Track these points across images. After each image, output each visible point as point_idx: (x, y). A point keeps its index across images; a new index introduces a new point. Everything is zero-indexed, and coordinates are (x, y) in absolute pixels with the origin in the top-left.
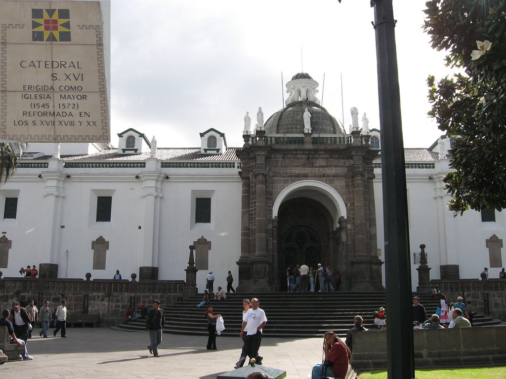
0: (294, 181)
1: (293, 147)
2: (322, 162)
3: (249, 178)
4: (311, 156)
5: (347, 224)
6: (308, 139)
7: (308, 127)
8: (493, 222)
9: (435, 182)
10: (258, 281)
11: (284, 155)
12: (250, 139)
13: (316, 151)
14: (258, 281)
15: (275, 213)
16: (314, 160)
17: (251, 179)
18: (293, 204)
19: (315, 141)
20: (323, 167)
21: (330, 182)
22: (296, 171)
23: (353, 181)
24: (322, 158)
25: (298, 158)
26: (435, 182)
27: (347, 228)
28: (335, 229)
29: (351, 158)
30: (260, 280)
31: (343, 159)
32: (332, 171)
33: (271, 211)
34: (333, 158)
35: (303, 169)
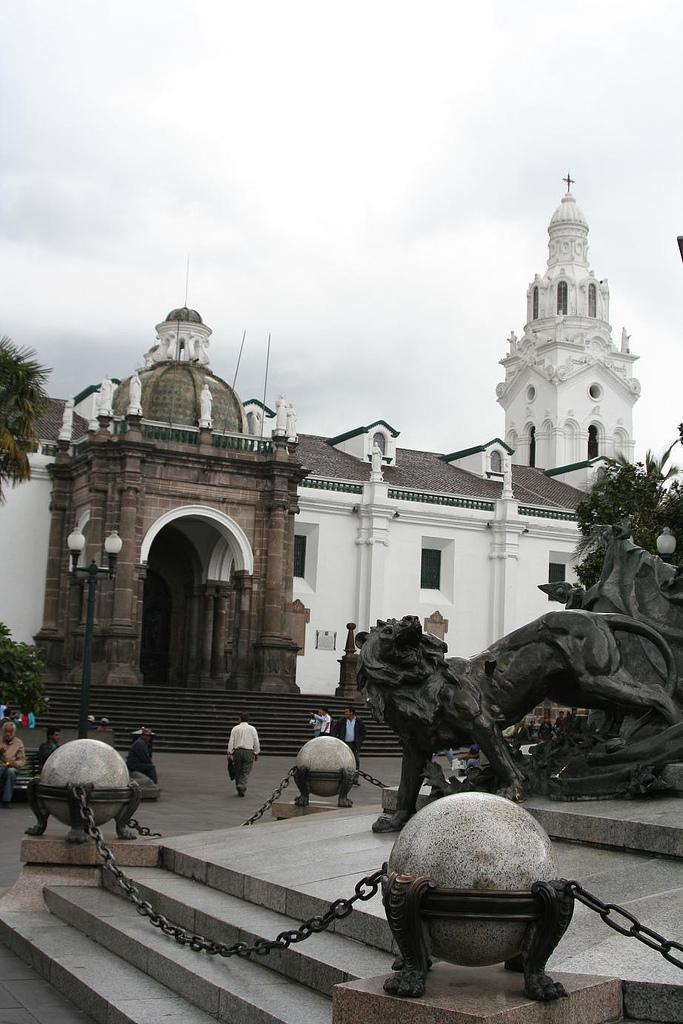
0: (178, 504)
1: (181, 447)
2: (223, 479)
3: (106, 492)
5: (252, 583)
6: (205, 437)
7: (206, 420)
8: (435, 591)
9: (360, 518)
10: (117, 666)
11: (168, 459)
12: (111, 424)
13: (218, 460)
14: (117, 666)
15: (144, 556)
16: (212, 474)
17: (110, 493)
19: (218, 442)
20: (226, 487)
21: (233, 513)
22: (183, 488)
23: (269, 516)
24: (225, 472)
25: (187, 467)
26: (360, 518)
27: (251, 589)
28: (204, 582)
29: (271, 478)
30: (121, 665)
31: (256, 477)
32: (238, 495)
33: (139, 551)
34: (241, 474)
35: (195, 486)
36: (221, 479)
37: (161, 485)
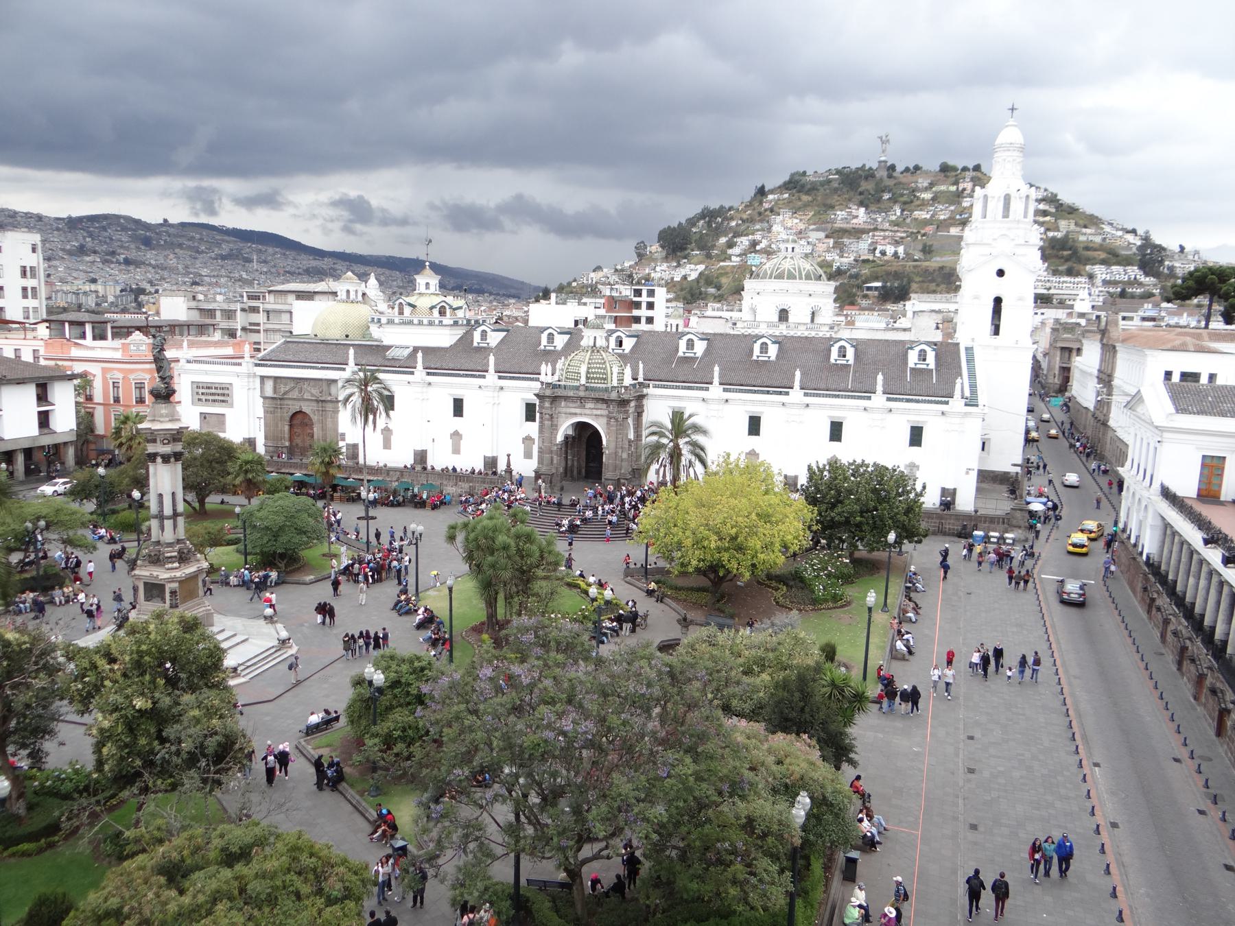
4: (582, 400)
15: (560, 438)
18: (582, 427)
22: (573, 410)
32: (599, 412)
36: (590, 405)
37: (564, 410)
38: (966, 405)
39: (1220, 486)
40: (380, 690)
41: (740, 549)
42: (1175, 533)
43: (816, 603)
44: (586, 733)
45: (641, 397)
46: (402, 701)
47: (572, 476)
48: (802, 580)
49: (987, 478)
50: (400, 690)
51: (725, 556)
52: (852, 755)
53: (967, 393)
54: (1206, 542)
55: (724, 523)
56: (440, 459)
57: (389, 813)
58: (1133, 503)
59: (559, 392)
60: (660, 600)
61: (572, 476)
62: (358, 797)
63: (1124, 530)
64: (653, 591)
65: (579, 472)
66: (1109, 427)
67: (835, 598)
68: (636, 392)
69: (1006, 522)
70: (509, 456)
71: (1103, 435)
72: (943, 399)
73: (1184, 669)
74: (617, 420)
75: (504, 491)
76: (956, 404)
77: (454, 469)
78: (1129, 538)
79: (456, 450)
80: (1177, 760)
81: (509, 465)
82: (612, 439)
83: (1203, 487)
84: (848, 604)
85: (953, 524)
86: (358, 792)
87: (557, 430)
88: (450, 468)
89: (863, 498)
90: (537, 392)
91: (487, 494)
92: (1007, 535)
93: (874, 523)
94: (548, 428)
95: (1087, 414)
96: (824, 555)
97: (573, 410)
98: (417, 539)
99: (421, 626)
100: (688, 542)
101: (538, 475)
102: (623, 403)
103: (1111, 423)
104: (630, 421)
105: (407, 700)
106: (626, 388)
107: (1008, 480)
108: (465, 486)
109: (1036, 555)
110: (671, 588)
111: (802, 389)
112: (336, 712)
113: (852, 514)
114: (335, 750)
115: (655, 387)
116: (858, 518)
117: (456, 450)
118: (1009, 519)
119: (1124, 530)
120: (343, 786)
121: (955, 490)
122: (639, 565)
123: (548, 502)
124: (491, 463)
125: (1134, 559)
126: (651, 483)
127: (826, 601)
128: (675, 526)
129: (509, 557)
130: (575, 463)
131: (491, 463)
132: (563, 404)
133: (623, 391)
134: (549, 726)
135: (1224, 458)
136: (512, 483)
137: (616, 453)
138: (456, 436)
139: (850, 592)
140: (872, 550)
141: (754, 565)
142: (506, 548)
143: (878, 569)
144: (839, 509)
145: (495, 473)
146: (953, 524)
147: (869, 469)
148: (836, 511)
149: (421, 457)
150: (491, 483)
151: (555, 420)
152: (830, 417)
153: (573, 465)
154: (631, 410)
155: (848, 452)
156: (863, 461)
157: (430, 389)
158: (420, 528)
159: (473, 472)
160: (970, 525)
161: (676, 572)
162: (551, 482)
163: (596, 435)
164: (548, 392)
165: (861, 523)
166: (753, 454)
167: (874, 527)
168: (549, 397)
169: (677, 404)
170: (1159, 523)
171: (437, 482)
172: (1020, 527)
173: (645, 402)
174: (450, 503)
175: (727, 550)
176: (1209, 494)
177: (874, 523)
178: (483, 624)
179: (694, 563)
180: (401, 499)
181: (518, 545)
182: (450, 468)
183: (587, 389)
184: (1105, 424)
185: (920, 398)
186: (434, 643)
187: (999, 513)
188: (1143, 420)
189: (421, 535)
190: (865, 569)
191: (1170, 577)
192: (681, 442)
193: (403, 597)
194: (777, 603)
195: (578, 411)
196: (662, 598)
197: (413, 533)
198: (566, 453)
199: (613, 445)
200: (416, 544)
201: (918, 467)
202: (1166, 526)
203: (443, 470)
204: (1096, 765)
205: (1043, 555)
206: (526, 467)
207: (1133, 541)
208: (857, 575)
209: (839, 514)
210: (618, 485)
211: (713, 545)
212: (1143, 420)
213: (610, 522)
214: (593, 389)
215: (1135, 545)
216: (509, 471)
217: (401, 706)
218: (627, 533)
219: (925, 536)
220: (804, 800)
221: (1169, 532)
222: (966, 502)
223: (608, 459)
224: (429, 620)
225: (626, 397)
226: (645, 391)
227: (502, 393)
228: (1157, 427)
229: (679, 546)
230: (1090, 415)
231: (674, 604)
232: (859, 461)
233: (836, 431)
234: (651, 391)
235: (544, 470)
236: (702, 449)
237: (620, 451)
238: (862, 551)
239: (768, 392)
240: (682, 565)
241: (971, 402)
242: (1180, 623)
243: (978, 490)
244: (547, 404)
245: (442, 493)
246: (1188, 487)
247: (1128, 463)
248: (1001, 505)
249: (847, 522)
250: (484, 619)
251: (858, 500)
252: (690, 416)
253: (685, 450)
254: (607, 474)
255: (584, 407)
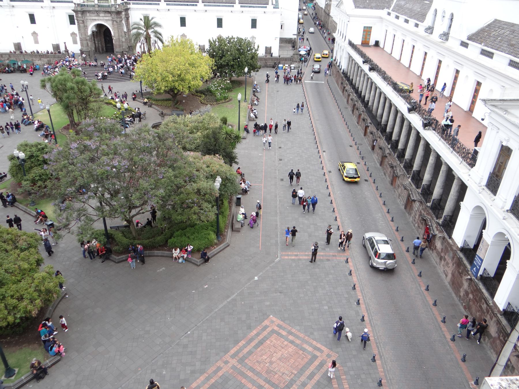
4: (97, 12)
15: (90, 33)
22: (94, 18)
33: (87, 32)
36: (102, 15)
37: (89, 18)
38: (274, 8)
39: (369, 39)
40: (24, 160)
41: (183, 80)
42: (353, 60)
43: (217, 100)
44: (125, 165)
45: (127, 10)
46: (36, 164)
47: (99, 51)
48: (211, 92)
49: (283, 41)
50: (34, 159)
51: (177, 84)
52: (236, 160)
53: (274, 3)
54: (364, 62)
55: (174, 69)
56: (28, 47)
57: (42, 211)
58: (338, 48)
59: (85, 9)
60: (150, 106)
61: (99, 51)
62: (25, 207)
63: (335, 60)
64: (146, 102)
65: (103, 50)
66: (330, 16)
67: (225, 98)
68: (124, 7)
69: (290, 60)
70: (65, 43)
71: (328, 19)
72: (265, 6)
73: (354, 112)
74: (117, 22)
75: (66, 61)
76: (270, 7)
77: (38, 52)
78: (337, 63)
79: (36, 42)
80: (351, 146)
81: (66, 48)
82: (116, 32)
83: (364, 40)
84: (231, 100)
85: (271, 63)
86: (25, 205)
87: (87, 29)
88: (36, 51)
89: (234, 53)
90: (73, 9)
91: (57, 63)
92: (292, 66)
93: (239, 64)
94: (83, 27)
95: (322, 10)
96: (219, 80)
97: (94, 18)
98: (26, 89)
99: (38, 129)
100: (159, 79)
101: (82, 52)
102: (119, 13)
103: (331, 14)
104: (123, 22)
105: (39, 163)
106: (119, 5)
107: (292, 42)
108: (46, 60)
109: (303, 73)
110: (154, 100)
111: (203, 2)
112: (4, 173)
113: (229, 61)
114: (8, 190)
115: (133, 4)
116: (232, 63)
117: (36, 42)
118: (292, 59)
119: (335, 60)
120: (16, 204)
121: (271, 47)
122: (138, 92)
123: (90, 65)
124: (56, 47)
125: (338, 71)
126: (138, 53)
127: (221, 100)
128: (152, 72)
129: (75, 93)
130: (100, 45)
131: (56, 47)
132: (88, 14)
133: (118, 7)
134: (108, 165)
135: (371, 27)
136: (70, 57)
137: (119, 39)
138: (34, 34)
139: (231, 95)
140: (239, 76)
141: (189, 87)
142: (72, 89)
143: (242, 84)
144: (223, 59)
145: (60, 52)
146: (271, 63)
147: (235, 40)
148: (222, 60)
149: (18, 46)
150: (59, 57)
151: (85, 23)
152: (217, 16)
153: (99, 46)
154: (123, 16)
155: (226, 33)
156: (232, 36)
157: (14, 9)
158: (26, 83)
159: (48, 52)
160: (277, 62)
161: (156, 93)
162: (89, 55)
163: (107, 30)
164: (79, 9)
165: (233, 64)
166: (183, 36)
167: (239, 66)
168: (80, 11)
169: (146, 13)
170: (347, 56)
171: (30, 59)
172: (296, 62)
173: (129, 12)
174: (39, 69)
175: (177, 81)
176: (365, 43)
177: (239, 64)
178: (69, 125)
179: (163, 88)
180: (12, 69)
181: (78, 87)
182: (36, 51)
183: (99, 6)
184: (328, 15)
185: (255, 5)
186: (46, 136)
187: (288, 56)
188: (343, 12)
189: (27, 86)
190: (236, 84)
191: (351, 78)
192: (150, 31)
193: (25, 117)
194: (201, 102)
195: (96, 18)
196: (151, 105)
197: (23, 85)
198: (94, 40)
199: (117, 35)
200: (26, 91)
201: (255, 38)
202: (350, 57)
203: (31, 53)
204: (324, 151)
205: (305, 73)
206: (75, 48)
207: (338, 64)
208: (233, 88)
209: (224, 61)
210: (122, 54)
211: (170, 79)
212: (343, 12)
213: (122, 73)
214: (102, 6)
215: (339, 66)
216: (67, 51)
217: (36, 166)
218: (131, 77)
219: (260, 68)
220: (219, 179)
221: (351, 59)
222: (276, 52)
223: (116, 42)
224: (41, 126)
225: (119, 10)
226: (129, 6)
227: (54, 10)
228: (348, 15)
229: (155, 81)
230: (323, 11)
231: (156, 108)
232: (230, 37)
233: (220, 24)
234: (131, 6)
235: (85, 49)
236: (160, 34)
237: (121, 38)
238: (235, 77)
239: (187, 5)
240: (158, 89)
241: (276, 7)
242: (354, 96)
243: (280, 47)
244: (80, 15)
245: (33, 65)
246: (358, 41)
247: (337, 32)
248: (289, 53)
249: (228, 65)
250: (69, 123)
251: (231, 54)
252: (152, 18)
253: (152, 35)
254: (116, 49)
255: (99, 16)
